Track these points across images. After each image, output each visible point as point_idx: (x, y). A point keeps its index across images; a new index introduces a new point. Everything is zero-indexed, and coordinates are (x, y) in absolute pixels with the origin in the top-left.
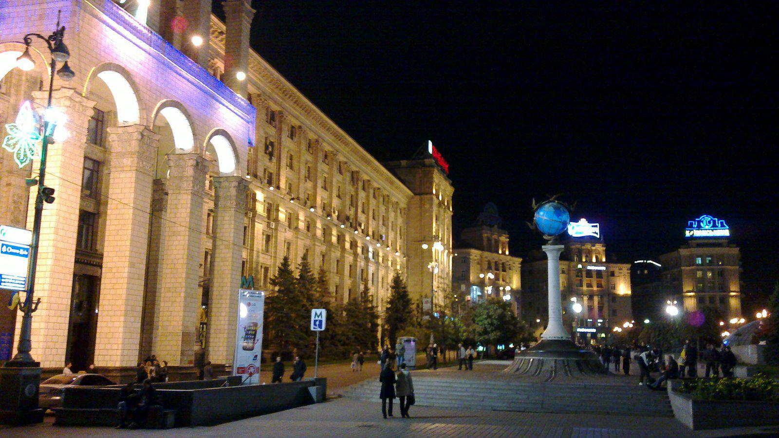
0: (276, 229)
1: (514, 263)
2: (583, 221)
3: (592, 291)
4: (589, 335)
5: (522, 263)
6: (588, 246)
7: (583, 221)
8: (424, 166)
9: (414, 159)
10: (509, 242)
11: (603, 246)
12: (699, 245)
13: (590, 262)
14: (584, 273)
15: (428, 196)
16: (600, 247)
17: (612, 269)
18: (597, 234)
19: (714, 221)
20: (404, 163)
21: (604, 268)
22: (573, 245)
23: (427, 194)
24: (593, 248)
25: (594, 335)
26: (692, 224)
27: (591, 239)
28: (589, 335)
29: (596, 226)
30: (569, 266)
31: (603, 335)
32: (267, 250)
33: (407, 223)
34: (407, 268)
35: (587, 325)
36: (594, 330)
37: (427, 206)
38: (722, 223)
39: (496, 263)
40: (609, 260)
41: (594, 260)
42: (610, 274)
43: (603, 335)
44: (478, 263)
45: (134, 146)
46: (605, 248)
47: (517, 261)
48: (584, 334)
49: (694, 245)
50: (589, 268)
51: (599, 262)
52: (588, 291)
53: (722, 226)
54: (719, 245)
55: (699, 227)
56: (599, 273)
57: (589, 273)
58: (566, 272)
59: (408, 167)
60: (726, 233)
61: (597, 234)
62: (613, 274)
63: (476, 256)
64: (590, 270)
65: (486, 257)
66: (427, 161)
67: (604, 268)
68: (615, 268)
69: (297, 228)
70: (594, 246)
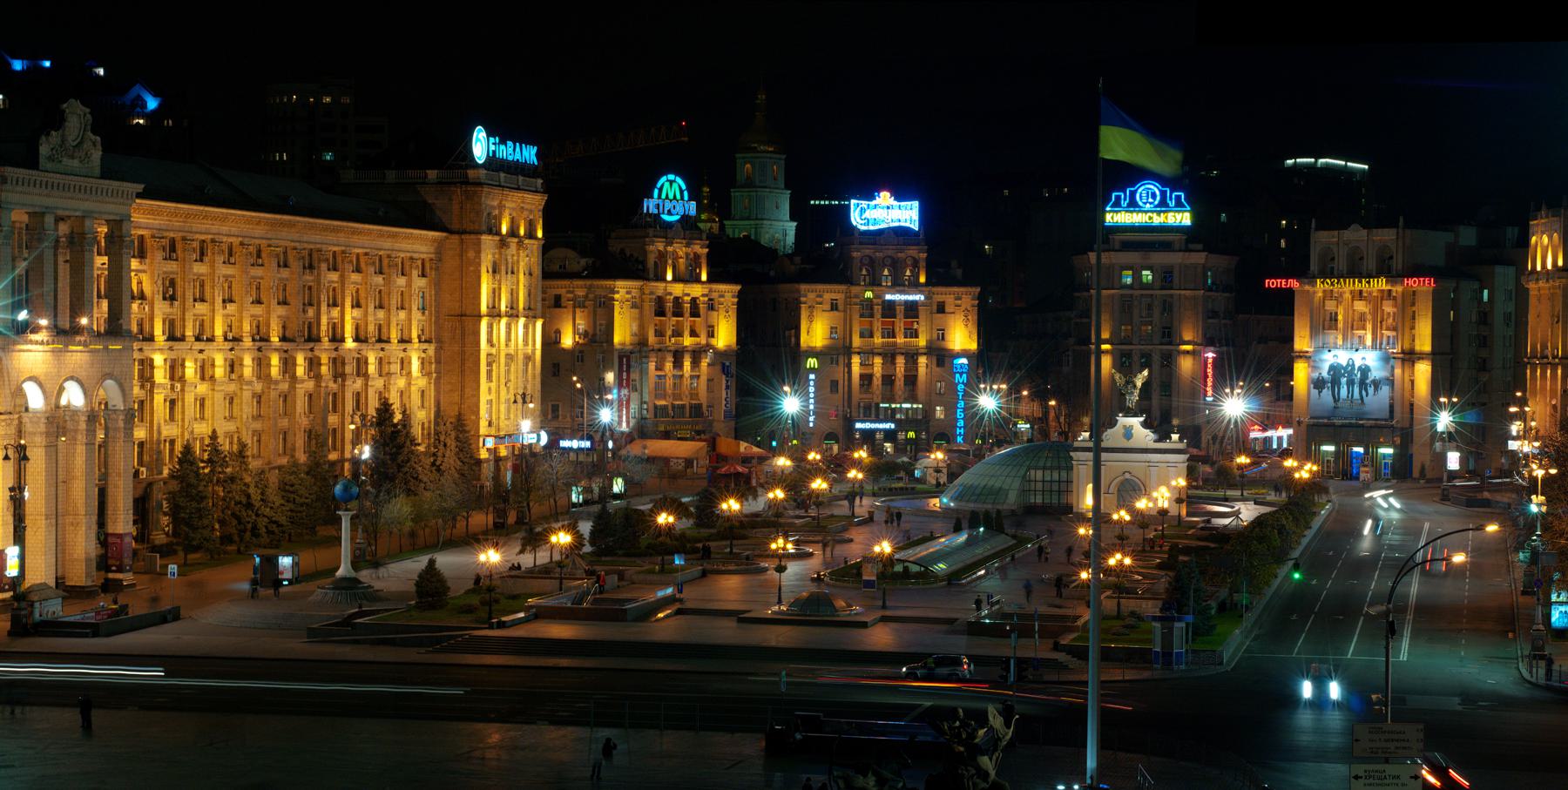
0: (183, 390)
2: (885, 198)
5: (740, 295)
7: (885, 198)
8: (466, 182)
12: (1128, 246)
14: (878, 309)
17: (940, 298)
19: (1163, 194)
20: (432, 174)
21: (919, 297)
25: (890, 436)
26: (1118, 198)
30: (848, 297)
31: (911, 434)
32: (172, 418)
33: (437, 285)
34: (438, 362)
35: (877, 416)
36: (890, 426)
37: (471, 254)
38: (1178, 198)
39: (677, 299)
43: (911, 434)
44: (634, 306)
45: (42, 428)
47: (728, 292)
48: (872, 432)
50: (888, 297)
53: (1179, 204)
54: (1166, 246)
55: (1133, 204)
56: (911, 308)
57: (889, 309)
58: (841, 307)
60: (1184, 218)
62: (941, 309)
64: (892, 303)
67: (919, 297)
68: (947, 295)
69: (212, 377)
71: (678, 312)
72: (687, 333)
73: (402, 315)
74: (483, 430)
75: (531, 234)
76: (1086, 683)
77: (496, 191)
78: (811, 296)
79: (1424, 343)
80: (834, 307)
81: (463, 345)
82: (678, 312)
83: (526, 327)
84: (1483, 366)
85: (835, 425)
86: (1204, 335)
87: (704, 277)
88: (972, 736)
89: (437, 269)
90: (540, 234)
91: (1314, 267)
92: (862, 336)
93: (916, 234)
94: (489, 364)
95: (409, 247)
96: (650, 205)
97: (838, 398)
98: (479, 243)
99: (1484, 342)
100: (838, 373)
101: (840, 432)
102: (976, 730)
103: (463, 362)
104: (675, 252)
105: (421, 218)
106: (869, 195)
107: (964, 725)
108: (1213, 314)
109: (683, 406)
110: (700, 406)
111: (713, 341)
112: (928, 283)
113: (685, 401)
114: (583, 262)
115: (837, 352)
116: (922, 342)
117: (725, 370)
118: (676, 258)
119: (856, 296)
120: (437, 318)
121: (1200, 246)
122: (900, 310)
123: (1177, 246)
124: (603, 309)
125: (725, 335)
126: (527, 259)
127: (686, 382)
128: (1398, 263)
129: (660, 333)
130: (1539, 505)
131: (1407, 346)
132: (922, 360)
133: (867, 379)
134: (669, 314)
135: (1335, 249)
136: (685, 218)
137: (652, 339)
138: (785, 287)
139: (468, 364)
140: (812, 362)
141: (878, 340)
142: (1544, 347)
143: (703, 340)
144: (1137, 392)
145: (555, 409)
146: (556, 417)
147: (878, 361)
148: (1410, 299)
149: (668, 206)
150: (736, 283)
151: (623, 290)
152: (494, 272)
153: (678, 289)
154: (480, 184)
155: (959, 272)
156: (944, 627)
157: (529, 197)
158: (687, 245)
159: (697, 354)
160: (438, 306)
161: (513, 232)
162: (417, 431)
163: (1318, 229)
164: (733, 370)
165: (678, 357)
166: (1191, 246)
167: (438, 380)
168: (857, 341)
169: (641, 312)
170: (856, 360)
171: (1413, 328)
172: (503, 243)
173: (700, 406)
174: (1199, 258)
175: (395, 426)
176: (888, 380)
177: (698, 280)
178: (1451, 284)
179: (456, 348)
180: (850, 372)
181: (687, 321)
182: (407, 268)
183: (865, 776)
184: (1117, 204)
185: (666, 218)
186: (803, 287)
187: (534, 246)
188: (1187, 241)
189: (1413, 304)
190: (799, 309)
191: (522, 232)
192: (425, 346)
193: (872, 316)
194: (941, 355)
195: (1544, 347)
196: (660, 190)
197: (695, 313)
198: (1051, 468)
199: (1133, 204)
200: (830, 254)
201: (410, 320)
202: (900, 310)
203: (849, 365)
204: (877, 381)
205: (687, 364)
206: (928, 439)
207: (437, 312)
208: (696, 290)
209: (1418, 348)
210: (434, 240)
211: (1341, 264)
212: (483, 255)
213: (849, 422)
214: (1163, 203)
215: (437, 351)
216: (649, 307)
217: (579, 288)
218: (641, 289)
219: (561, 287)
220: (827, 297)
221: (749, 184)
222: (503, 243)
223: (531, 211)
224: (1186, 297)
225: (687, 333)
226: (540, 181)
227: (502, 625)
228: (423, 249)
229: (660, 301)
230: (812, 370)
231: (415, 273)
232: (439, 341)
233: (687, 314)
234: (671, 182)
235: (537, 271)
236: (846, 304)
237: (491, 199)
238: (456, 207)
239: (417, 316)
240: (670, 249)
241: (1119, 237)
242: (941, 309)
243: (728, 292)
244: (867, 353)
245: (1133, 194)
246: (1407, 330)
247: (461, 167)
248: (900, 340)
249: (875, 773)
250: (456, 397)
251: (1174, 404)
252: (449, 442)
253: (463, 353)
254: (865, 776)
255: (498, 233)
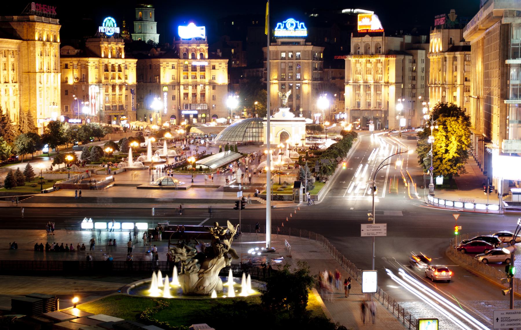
1: (130, 64)
3: (197, 81)
4: (191, 116)
5: (137, 63)
6: (194, 46)
7: (192, 25)
8: (29, 21)
9: (22, 15)
10: (125, 48)
11: (206, 46)
12: (283, 44)
13: (194, 57)
14: (190, 68)
15: (32, 42)
16: (204, 47)
18: (203, 35)
19: (296, 24)
20: (15, 18)
22: (182, 46)
23: (31, 40)
24: (198, 48)
25: (195, 116)
26: (280, 26)
27: (199, 40)
28: (191, 116)
29: (203, 29)
30: (178, 63)
33: (19, 60)
34: (20, 90)
36: (196, 112)
37: (32, 49)
38: (302, 26)
39: (113, 65)
40: (211, 57)
41: (198, 57)
42: (211, 67)
43: (204, 115)
44: (96, 68)
46: (207, 47)
47: (132, 63)
49: (280, 44)
51: (202, 57)
52: (193, 82)
53: (302, 27)
54: (298, 44)
56: (203, 69)
57: (194, 69)
58: (176, 67)
59: (18, 21)
61: (203, 35)
62: (214, 68)
63: (94, 63)
65: (103, 63)
66: (31, 17)
68: (215, 62)
70: (199, 46)
71: (113, 70)
72: (117, 78)
73: (6, 72)
74: (38, 116)
75: (55, 41)
76: (266, 209)
77: (41, 24)
78: (165, 63)
79: (392, 78)
80: (173, 68)
81: (30, 84)
82: (113, 70)
83: (54, 76)
84: (414, 87)
85: (174, 112)
86: (312, 77)
87: (123, 56)
88: (221, 232)
89: (18, 54)
90: (59, 40)
91: (352, 51)
92: (184, 78)
93: (204, 40)
94: (40, 91)
95: (7, 46)
96: (101, 29)
97: (176, 102)
98: (34, 44)
99: (414, 78)
100: (176, 92)
101: (177, 116)
102: (223, 230)
103: (30, 90)
104: (111, 47)
105: (12, 35)
106: (186, 23)
107: (219, 229)
108: (316, 69)
109: (116, 106)
110: (122, 106)
111: (127, 81)
112: (209, 58)
113: (117, 104)
114: (76, 51)
115: (175, 85)
116: (207, 80)
117: (132, 92)
118: (112, 49)
119: (182, 63)
120: (19, 73)
121: (310, 44)
122: (198, 68)
123: (302, 43)
124: (85, 68)
125: (132, 79)
126: (54, 49)
127: (117, 96)
128: (383, 50)
129: (106, 78)
130: (432, 140)
131: (386, 81)
132: (207, 87)
133: (186, 95)
134: (110, 70)
135: (360, 44)
136: (115, 34)
137: (103, 80)
138: (154, 60)
139: (32, 91)
140: (165, 89)
141: (190, 80)
142: (435, 80)
143: (123, 80)
144: (287, 99)
145: (67, 108)
146: (67, 110)
147: (190, 87)
148: (387, 63)
149: (109, 29)
150: (135, 58)
151: (92, 62)
152: (41, 55)
153: (113, 61)
154: (35, 21)
155: (220, 54)
156: (216, 189)
157: (54, 26)
158: (116, 44)
159: (121, 86)
160: (19, 69)
161: (48, 40)
162: (12, 118)
163: (354, 36)
164: (135, 92)
165: (114, 87)
166: (307, 43)
167: (20, 97)
168: (182, 81)
169: (99, 70)
170: (182, 87)
171: (388, 73)
172: (44, 44)
173: (122, 106)
174: (310, 48)
175: (3, 115)
176: (194, 95)
177: (121, 58)
178: (401, 57)
179: (27, 85)
180: (179, 92)
181: (117, 73)
182: (7, 54)
183: (182, 248)
184: (279, 27)
185: (108, 34)
186: (161, 60)
187: (57, 45)
188: (306, 42)
189: (388, 65)
190: (159, 69)
191: (51, 40)
192: (15, 84)
193: (188, 71)
194: (213, 85)
195: (435, 80)
196: (105, 23)
197: (120, 71)
198: (255, 128)
199: (285, 27)
200: (170, 47)
201: (8, 74)
202: (198, 68)
203: (179, 89)
204: (190, 95)
205: (117, 88)
206: (210, 117)
207: (19, 71)
208: (120, 62)
209: (390, 82)
210: (17, 43)
211: (362, 50)
212: (36, 49)
213: (180, 111)
214: (296, 27)
215: (19, 86)
216: (102, 68)
217: (75, 61)
218: (99, 61)
219: (68, 61)
220: (171, 64)
221: (141, 20)
222: (44, 44)
223: (55, 32)
224: (305, 63)
225: (117, 78)
226: (58, 20)
227: (46, 192)
228: (13, 47)
229: (106, 66)
230: (165, 91)
231: (10, 56)
232: (21, 83)
233: (117, 70)
234: (110, 20)
235: (58, 55)
236: (178, 66)
237: (39, 27)
238: (25, 31)
239: (11, 72)
240: (110, 46)
241: (280, 40)
242: (214, 68)
243: (132, 63)
244: (186, 86)
245: (285, 24)
246: (386, 74)
247: (27, 15)
248: (198, 80)
249: (186, 247)
250: (27, 104)
251: (301, 103)
252: (25, 121)
253: (30, 87)
254: (182, 248)
255: (42, 40)
